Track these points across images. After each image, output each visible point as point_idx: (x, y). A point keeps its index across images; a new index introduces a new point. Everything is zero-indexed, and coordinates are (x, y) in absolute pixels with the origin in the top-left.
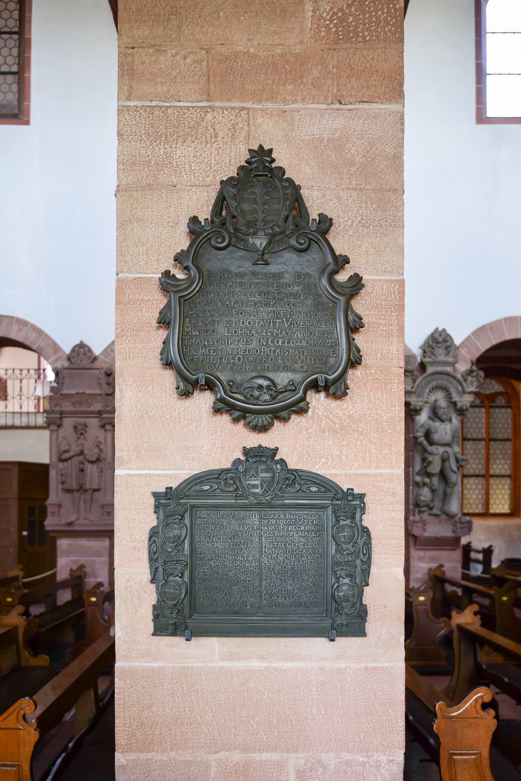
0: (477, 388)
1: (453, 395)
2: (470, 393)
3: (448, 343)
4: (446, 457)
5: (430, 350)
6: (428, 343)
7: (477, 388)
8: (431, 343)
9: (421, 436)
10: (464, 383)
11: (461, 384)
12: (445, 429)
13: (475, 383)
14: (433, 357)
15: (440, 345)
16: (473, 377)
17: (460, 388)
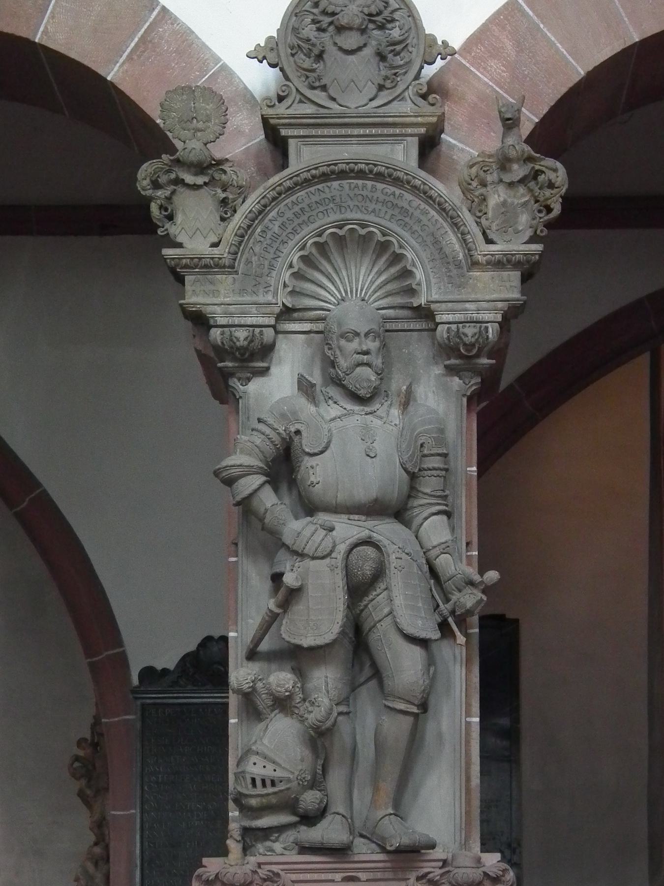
0: (532, 240)
1: (419, 274)
2: (499, 264)
3: (396, 34)
4: (368, 569)
5: (307, 63)
6: (295, 30)
7: (532, 240)
8: (309, 31)
9: (249, 471)
10: (468, 218)
11: (455, 225)
12: (366, 434)
13: (524, 219)
14: (319, 96)
15: (351, 40)
16: (511, 185)
17: (452, 240)
